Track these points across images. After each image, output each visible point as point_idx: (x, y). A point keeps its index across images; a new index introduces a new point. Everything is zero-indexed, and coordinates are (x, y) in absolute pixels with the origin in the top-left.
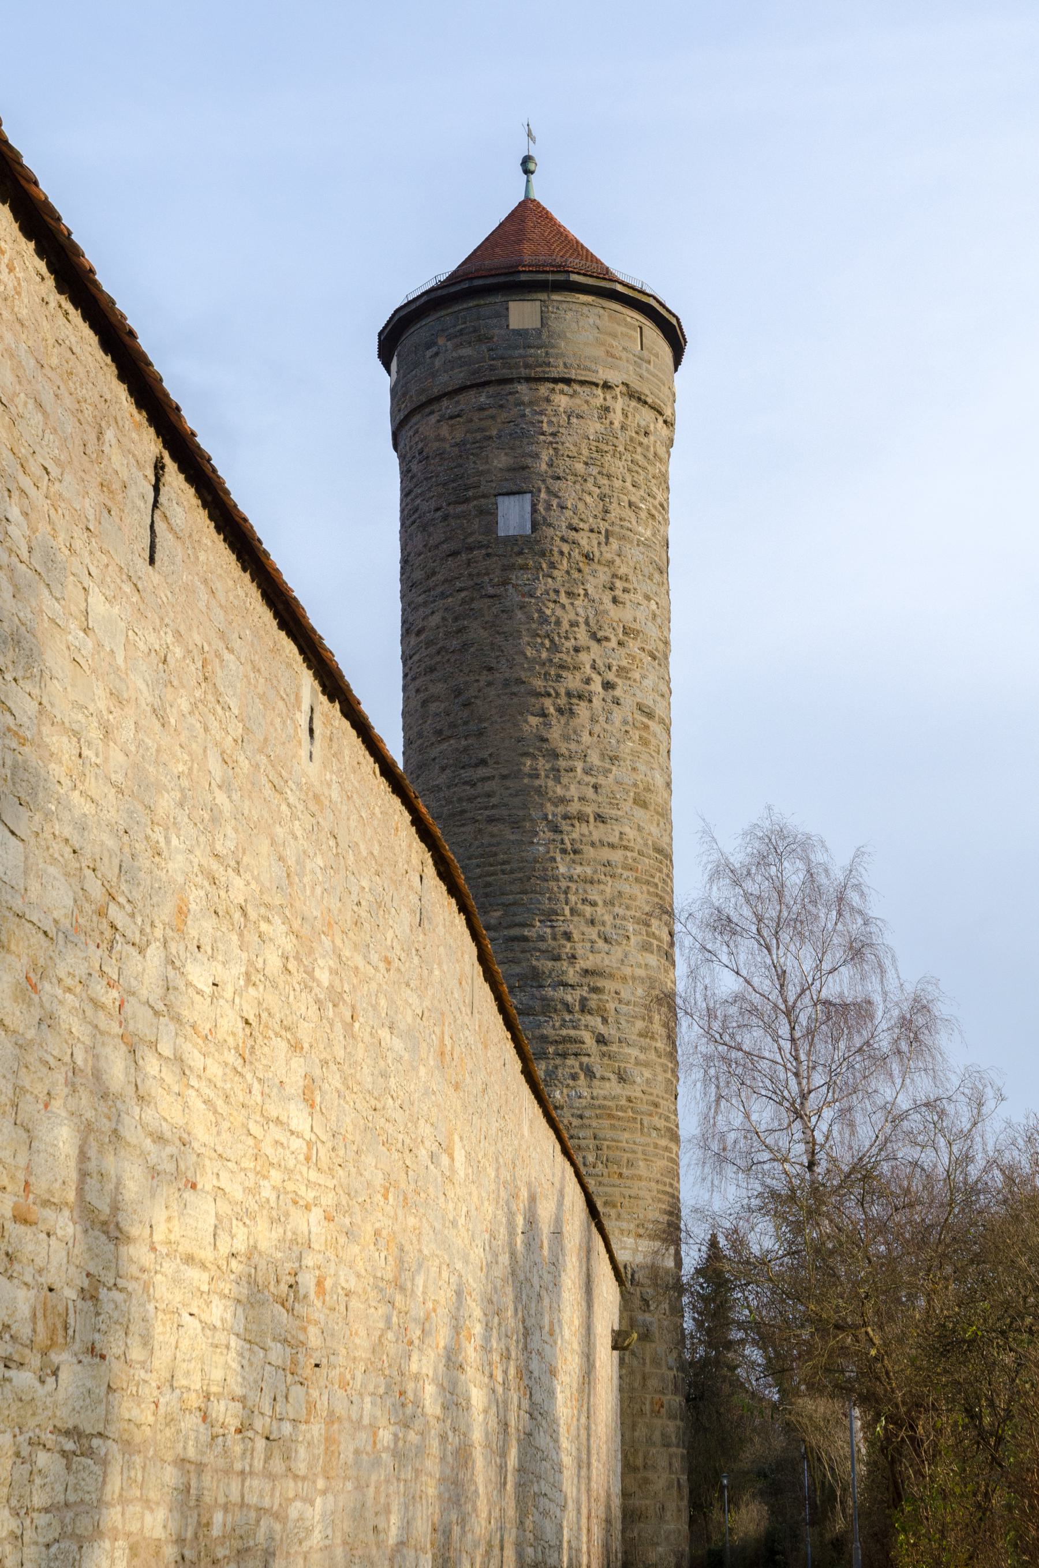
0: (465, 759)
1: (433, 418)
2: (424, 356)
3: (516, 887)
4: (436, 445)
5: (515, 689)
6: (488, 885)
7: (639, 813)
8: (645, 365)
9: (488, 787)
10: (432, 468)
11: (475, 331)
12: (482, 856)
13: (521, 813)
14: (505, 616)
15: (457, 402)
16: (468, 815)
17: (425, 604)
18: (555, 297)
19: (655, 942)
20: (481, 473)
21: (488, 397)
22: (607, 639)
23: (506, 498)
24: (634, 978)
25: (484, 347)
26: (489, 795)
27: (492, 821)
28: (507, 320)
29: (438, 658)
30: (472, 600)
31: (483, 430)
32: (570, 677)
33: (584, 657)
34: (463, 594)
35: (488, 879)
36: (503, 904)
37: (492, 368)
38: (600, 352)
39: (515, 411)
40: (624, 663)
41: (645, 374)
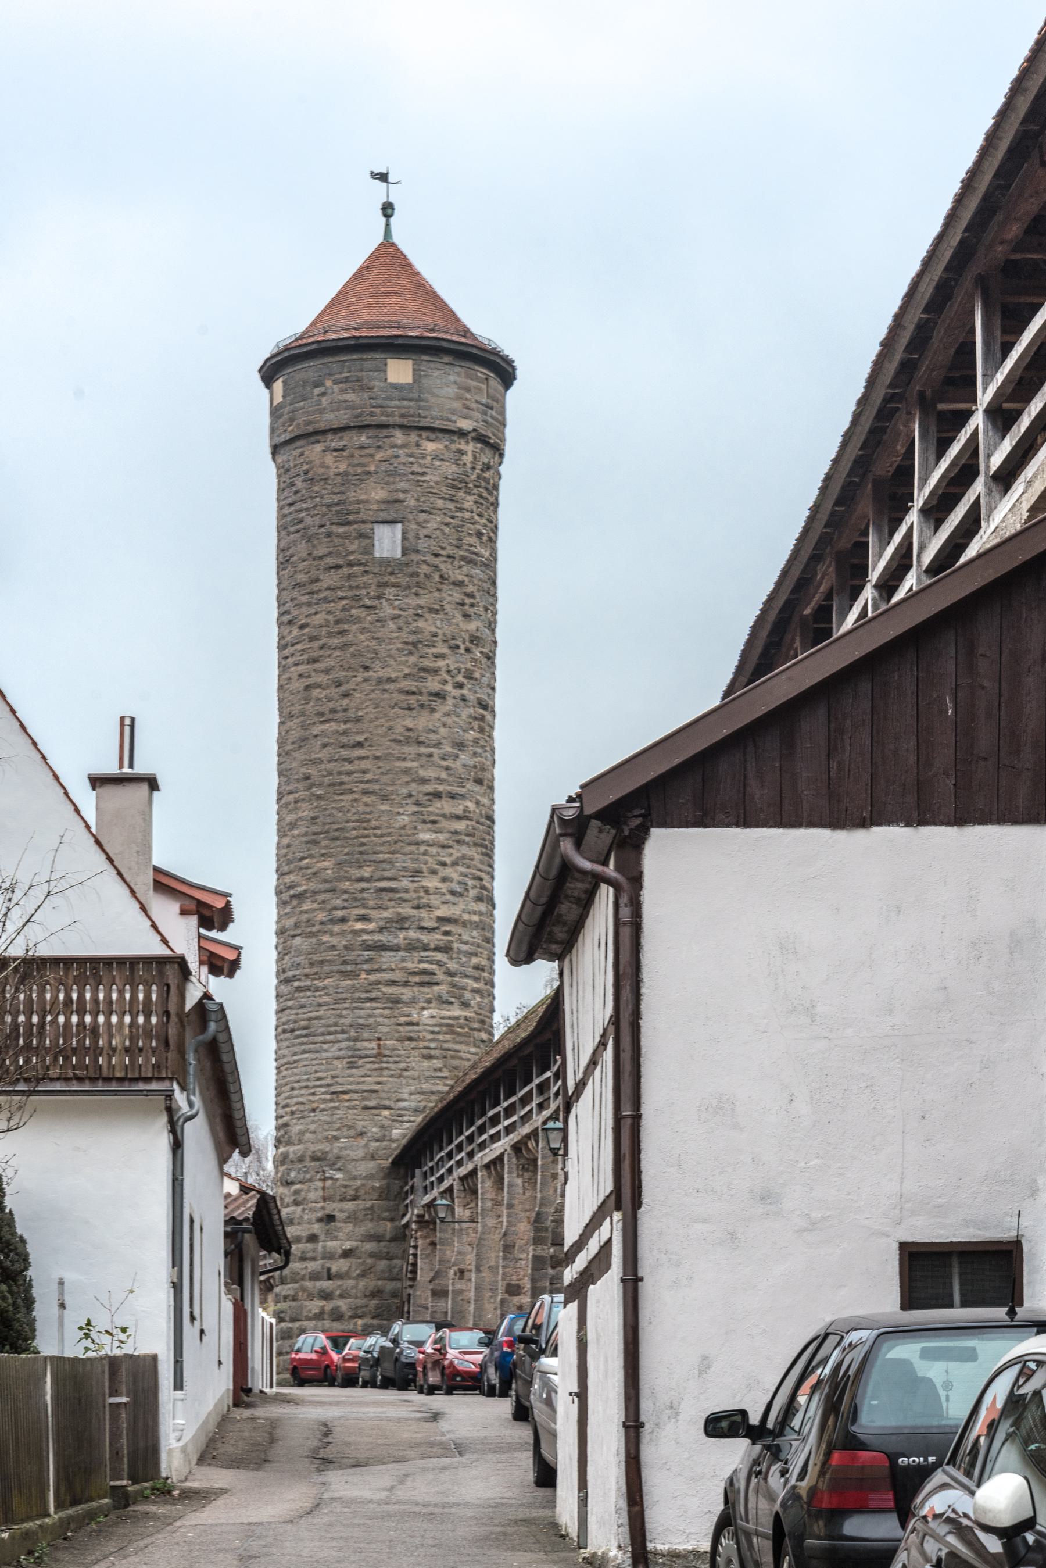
0: (344, 740)
1: (319, 448)
2: (312, 393)
4: (321, 470)
5: (387, 687)
6: (363, 844)
7: (477, 788)
8: (490, 411)
9: (363, 765)
10: (316, 488)
11: (358, 381)
12: (357, 821)
13: (390, 788)
14: (379, 624)
15: (341, 438)
17: (309, 604)
19: (485, 893)
21: (368, 438)
22: (458, 647)
23: (381, 526)
24: (471, 923)
25: (366, 396)
26: (364, 772)
28: (386, 374)
29: (322, 652)
30: (352, 607)
31: (364, 465)
32: (430, 678)
33: (441, 663)
34: (344, 602)
35: (364, 840)
36: (374, 861)
37: (372, 414)
39: (389, 452)
40: (469, 665)
41: (490, 420)
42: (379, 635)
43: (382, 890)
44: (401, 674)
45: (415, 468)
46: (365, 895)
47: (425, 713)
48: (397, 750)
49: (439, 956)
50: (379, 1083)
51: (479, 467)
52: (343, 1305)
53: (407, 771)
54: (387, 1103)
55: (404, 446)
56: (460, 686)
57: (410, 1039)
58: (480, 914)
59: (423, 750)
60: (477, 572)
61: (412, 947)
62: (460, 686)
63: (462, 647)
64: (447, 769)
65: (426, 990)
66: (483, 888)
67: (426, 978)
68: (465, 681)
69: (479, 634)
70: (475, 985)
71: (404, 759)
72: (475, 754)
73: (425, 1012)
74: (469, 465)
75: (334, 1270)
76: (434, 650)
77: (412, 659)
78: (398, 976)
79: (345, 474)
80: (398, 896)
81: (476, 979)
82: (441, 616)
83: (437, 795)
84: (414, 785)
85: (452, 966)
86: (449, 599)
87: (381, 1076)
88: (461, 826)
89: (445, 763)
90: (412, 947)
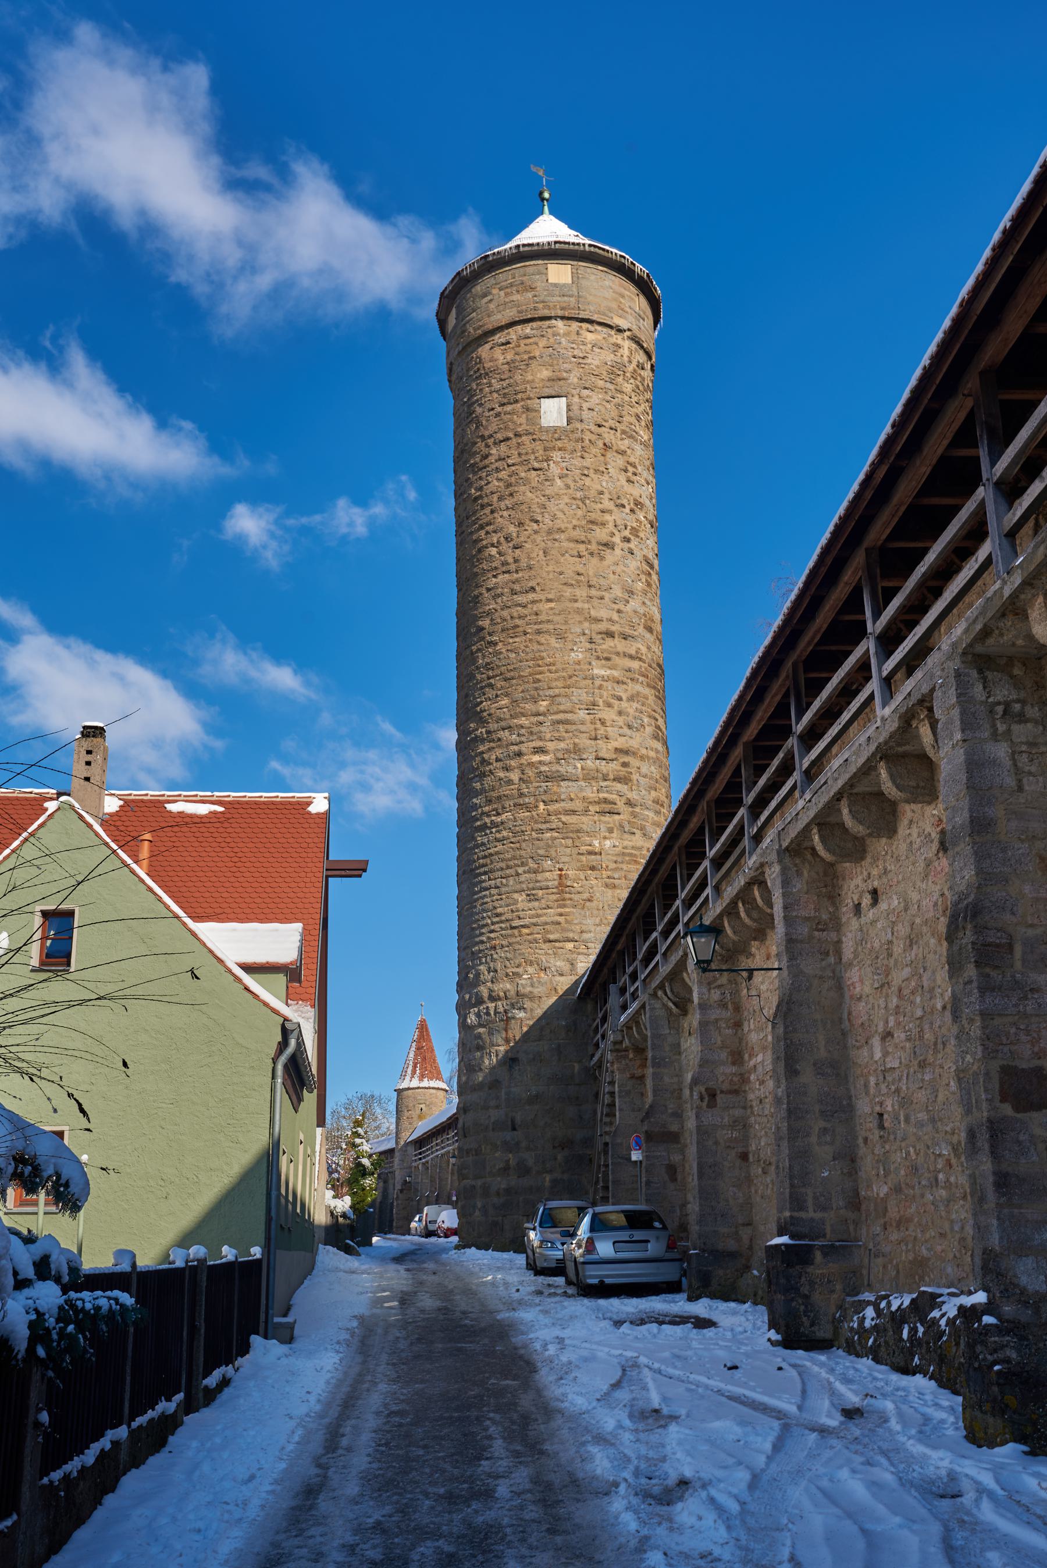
1: (487, 346)
3: (560, 684)
6: (539, 681)
7: (648, 635)
12: (533, 659)
14: (548, 483)
15: (508, 334)
16: (521, 629)
18: (581, 263)
20: (528, 382)
22: (623, 506)
24: (648, 758)
25: (530, 295)
27: (540, 633)
32: (598, 530)
33: (607, 517)
34: (513, 468)
36: (551, 696)
38: (614, 305)
40: (635, 525)
42: (547, 492)
43: (559, 722)
44: (570, 526)
45: (576, 353)
46: (543, 729)
47: (595, 561)
48: (568, 592)
49: (619, 786)
50: (561, 915)
51: (634, 364)
52: (530, 1159)
53: (579, 611)
54: (571, 935)
55: (567, 334)
56: (627, 540)
57: (593, 868)
58: (657, 751)
59: (593, 592)
60: (638, 447)
61: (589, 777)
62: (628, 540)
63: (628, 507)
64: (619, 611)
65: (607, 818)
66: (658, 727)
67: (607, 807)
68: (632, 538)
69: (641, 500)
70: (656, 818)
71: (576, 601)
72: (644, 603)
73: (608, 843)
74: (626, 359)
75: (518, 1119)
76: (600, 506)
77: (580, 513)
78: (578, 805)
79: (513, 361)
80: (574, 727)
81: (658, 813)
82: (606, 477)
83: (610, 635)
84: (586, 625)
85: (633, 796)
86: (613, 464)
87: (564, 906)
88: (635, 665)
89: (616, 607)
90: (589, 777)
